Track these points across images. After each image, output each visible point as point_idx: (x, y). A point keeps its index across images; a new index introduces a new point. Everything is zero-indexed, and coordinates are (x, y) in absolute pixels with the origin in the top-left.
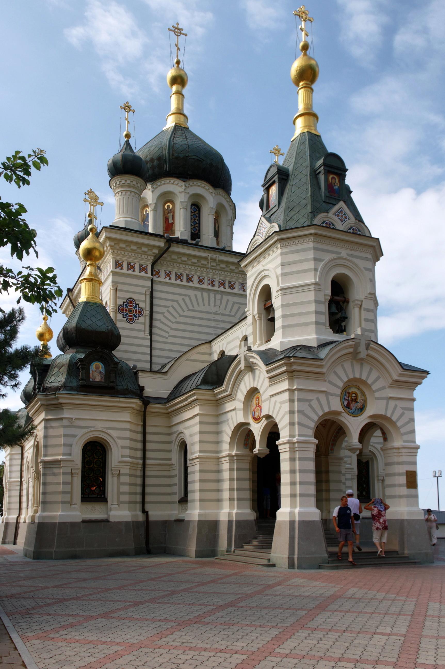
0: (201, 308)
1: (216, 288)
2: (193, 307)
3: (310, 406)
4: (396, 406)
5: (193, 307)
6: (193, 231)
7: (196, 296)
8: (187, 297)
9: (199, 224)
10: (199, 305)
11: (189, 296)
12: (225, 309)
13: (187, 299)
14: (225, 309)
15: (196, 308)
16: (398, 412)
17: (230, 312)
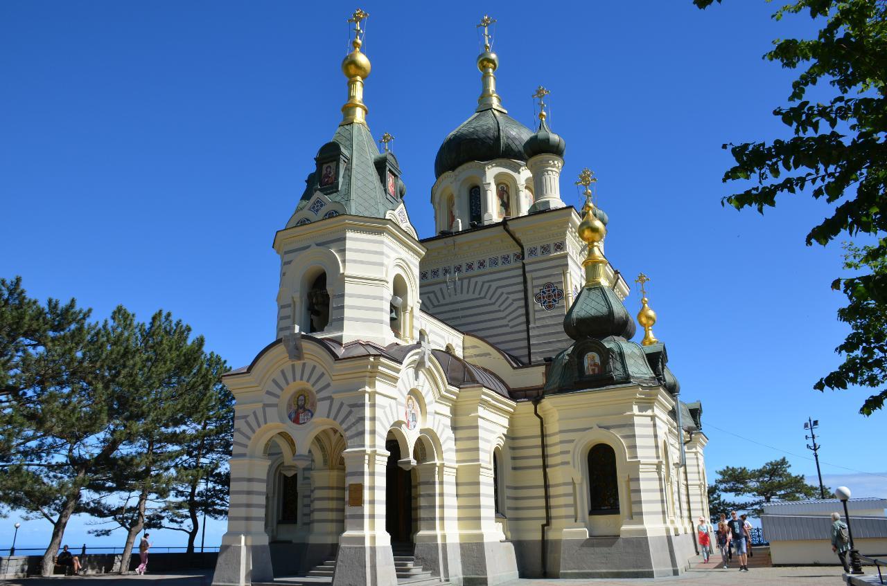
0: (448, 300)
1: (464, 273)
2: (439, 302)
3: (247, 423)
4: (342, 404)
5: (439, 302)
6: (474, 214)
7: (441, 289)
8: (432, 294)
9: (471, 206)
10: (444, 299)
11: (434, 292)
12: (474, 293)
13: (432, 296)
14: (474, 293)
15: (442, 302)
16: (345, 410)
17: (479, 294)
